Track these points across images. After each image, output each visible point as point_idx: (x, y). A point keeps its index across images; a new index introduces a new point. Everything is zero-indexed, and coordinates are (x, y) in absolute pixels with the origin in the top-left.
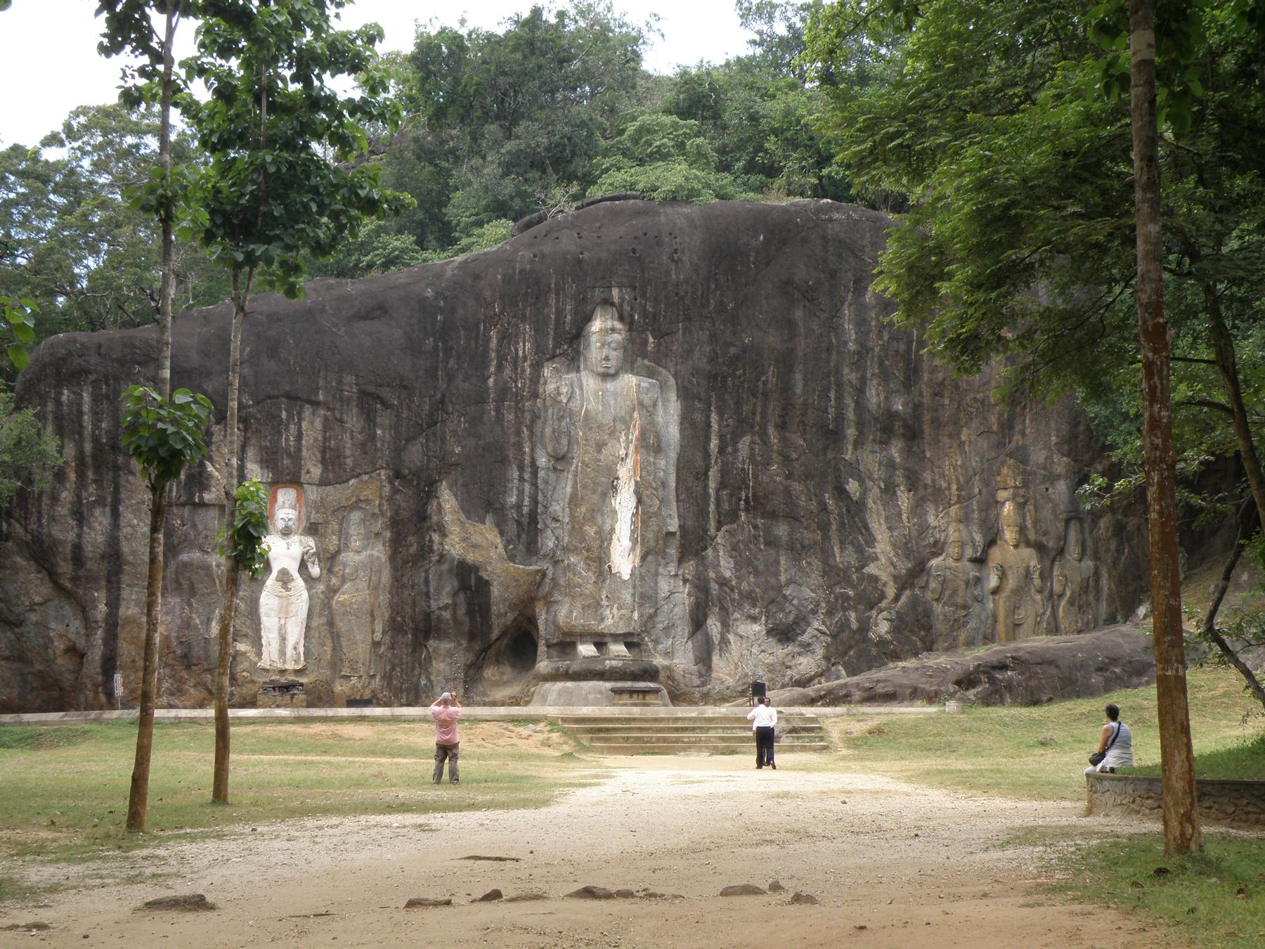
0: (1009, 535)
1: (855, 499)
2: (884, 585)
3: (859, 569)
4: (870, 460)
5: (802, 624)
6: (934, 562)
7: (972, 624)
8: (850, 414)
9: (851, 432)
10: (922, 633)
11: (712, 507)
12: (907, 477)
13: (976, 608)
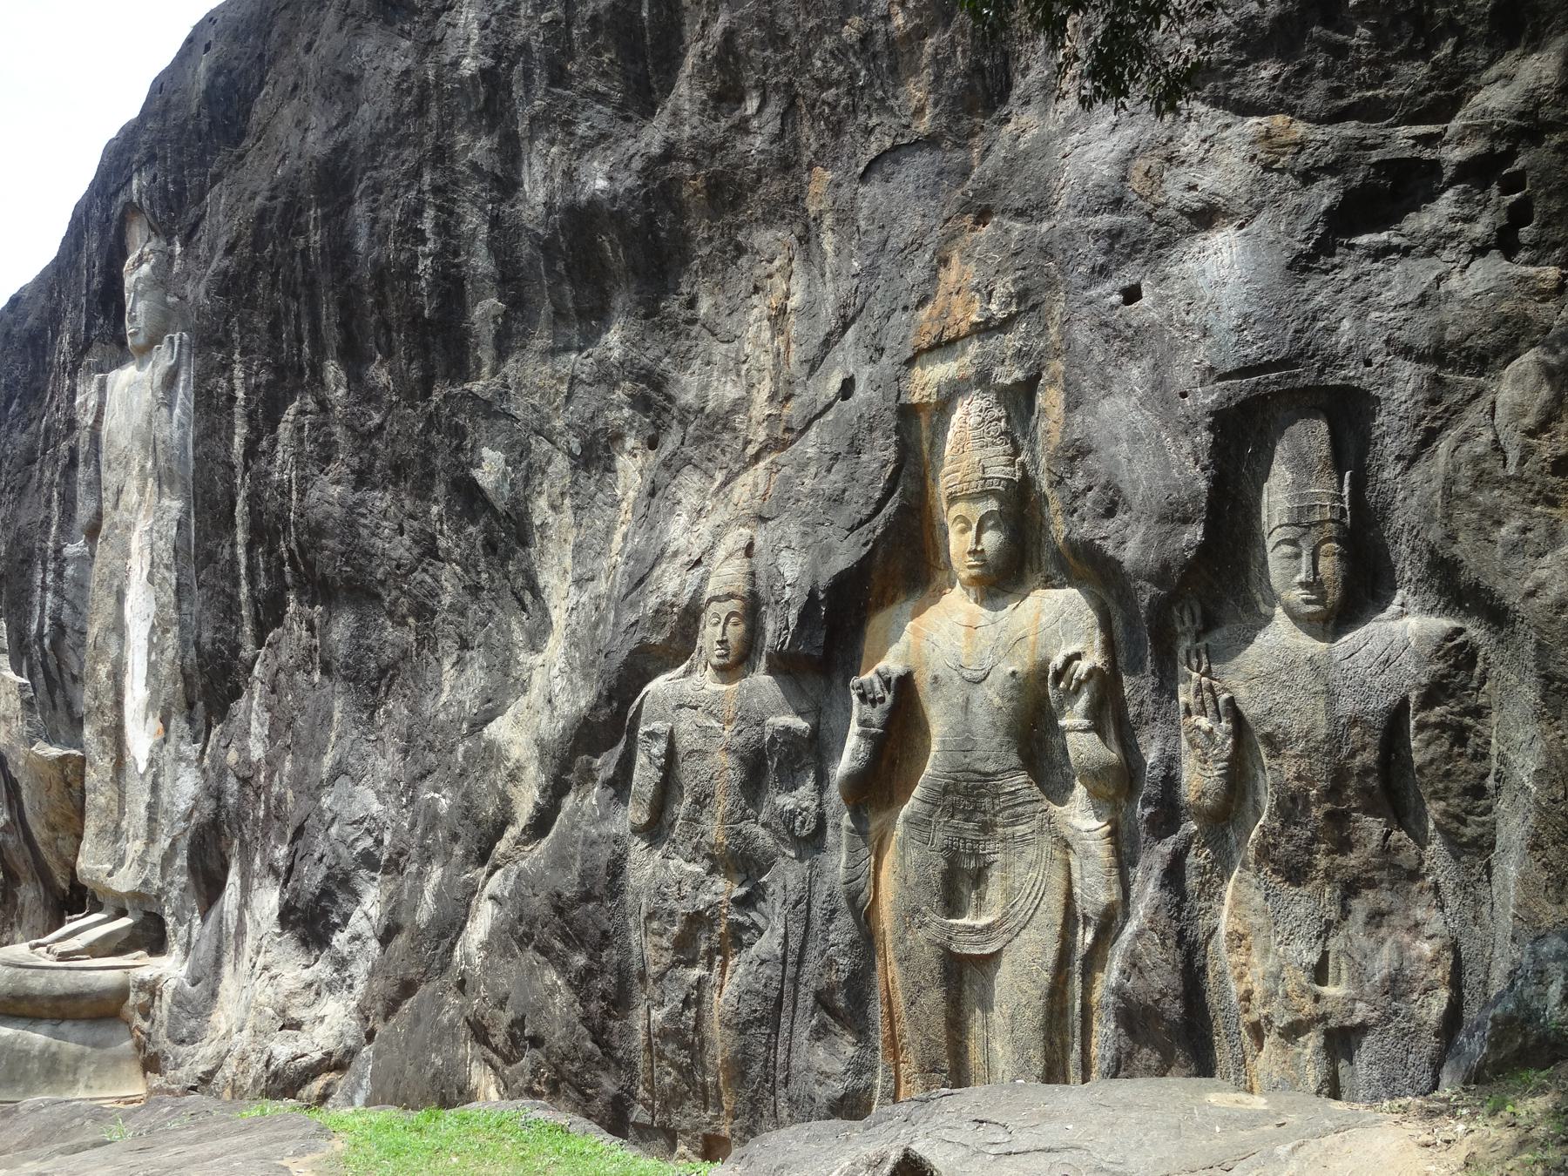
0: (964, 540)
1: (501, 506)
2: (514, 777)
3: (478, 724)
4: (538, 377)
5: (341, 897)
6: (659, 685)
7: (767, 944)
8: (481, 262)
9: (485, 309)
10: (580, 960)
11: (244, 589)
12: (641, 403)
13: (786, 875)
